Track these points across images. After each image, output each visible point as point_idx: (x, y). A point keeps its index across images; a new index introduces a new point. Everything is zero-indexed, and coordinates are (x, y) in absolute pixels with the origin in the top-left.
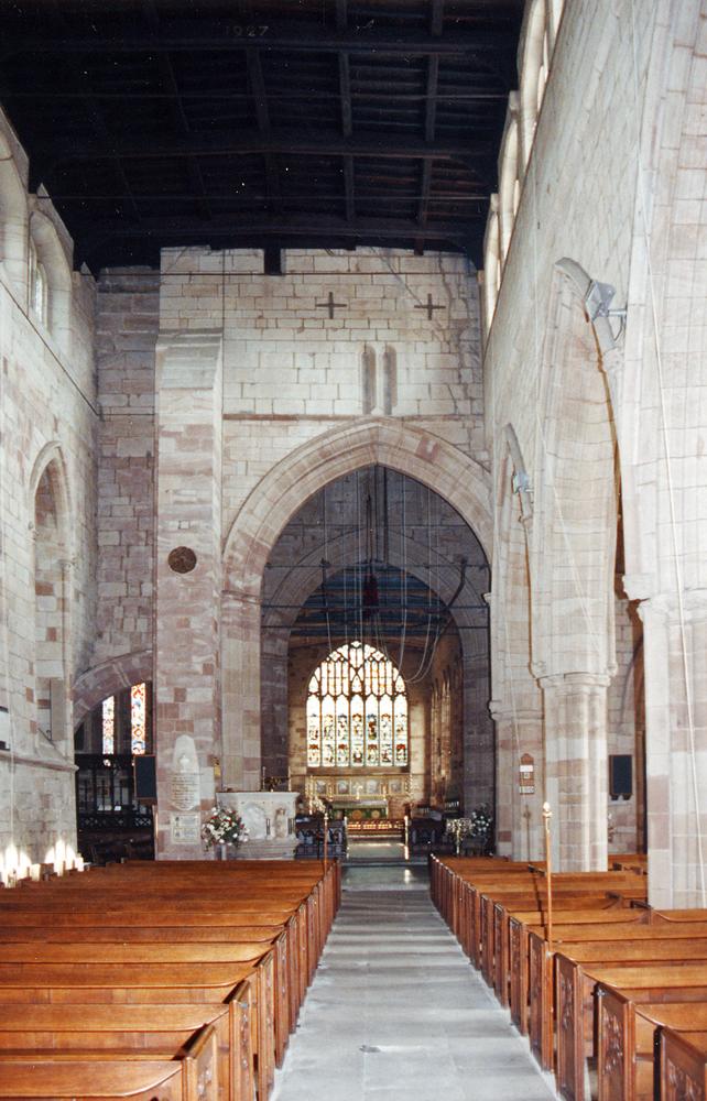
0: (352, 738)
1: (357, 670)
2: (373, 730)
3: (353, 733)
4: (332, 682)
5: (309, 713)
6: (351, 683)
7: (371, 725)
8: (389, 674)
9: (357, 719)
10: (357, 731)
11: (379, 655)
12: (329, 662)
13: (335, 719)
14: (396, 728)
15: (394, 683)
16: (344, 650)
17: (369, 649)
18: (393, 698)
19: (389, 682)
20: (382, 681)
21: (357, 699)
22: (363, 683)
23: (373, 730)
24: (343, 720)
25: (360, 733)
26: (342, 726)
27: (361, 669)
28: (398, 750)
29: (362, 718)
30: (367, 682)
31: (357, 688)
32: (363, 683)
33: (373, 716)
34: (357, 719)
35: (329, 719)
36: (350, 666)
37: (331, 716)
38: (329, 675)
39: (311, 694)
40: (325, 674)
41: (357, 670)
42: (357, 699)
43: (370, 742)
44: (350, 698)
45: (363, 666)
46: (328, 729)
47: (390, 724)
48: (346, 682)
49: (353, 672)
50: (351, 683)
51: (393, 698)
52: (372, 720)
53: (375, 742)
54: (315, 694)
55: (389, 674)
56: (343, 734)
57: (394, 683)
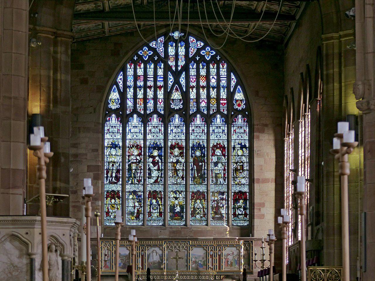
0: (170, 181)
1: (177, 75)
2: (199, 169)
3: (170, 173)
4: (140, 95)
5: (108, 139)
6: (168, 95)
7: (196, 161)
8: (224, 82)
9: (176, 152)
10: (176, 171)
11: (208, 53)
12: (136, 64)
13: (144, 150)
14: (233, 166)
15: (231, 95)
16: (158, 44)
17: (195, 44)
18: (229, 120)
19: (223, 95)
20: (213, 93)
21: (177, 120)
22: (185, 96)
23: (199, 169)
24: (155, 153)
25: (180, 174)
26: (155, 163)
27: (183, 75)
28: (236, 201)
29: (184, 150)
30: (193, 95)
31: (177, 106)
32: (185, 96)
33: (199, 147)
34: (176, 152)
35: (136, 152)
36: (167, 68)
37: (138, 147)
38: (136, 81)
39: (111, 111)
40: (130, 82)
41: (177, 75)
42: (177, 120)
43: (193, 188)
44: (165, 119)
45: (186, 68)
46: (134, 167)
47: (224, 160)
48: (161, 94)
49: (171, 79)
50: (168, 95)
51: (229, 120)
52: (198, 153)
53: (202, 188)
54: (116, 111)
55: (224, 82)
56: (155, 174)
57: (231, 95)
